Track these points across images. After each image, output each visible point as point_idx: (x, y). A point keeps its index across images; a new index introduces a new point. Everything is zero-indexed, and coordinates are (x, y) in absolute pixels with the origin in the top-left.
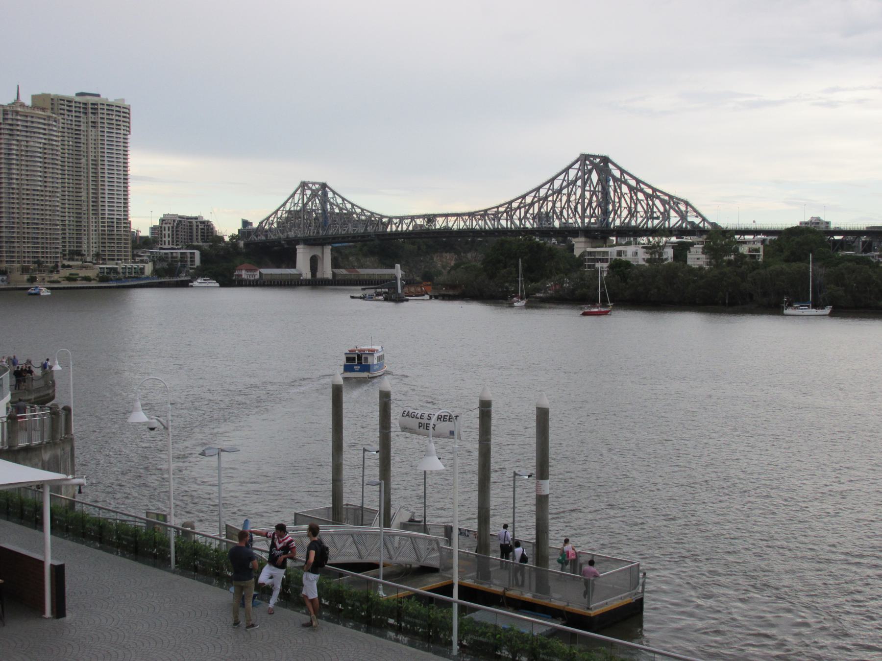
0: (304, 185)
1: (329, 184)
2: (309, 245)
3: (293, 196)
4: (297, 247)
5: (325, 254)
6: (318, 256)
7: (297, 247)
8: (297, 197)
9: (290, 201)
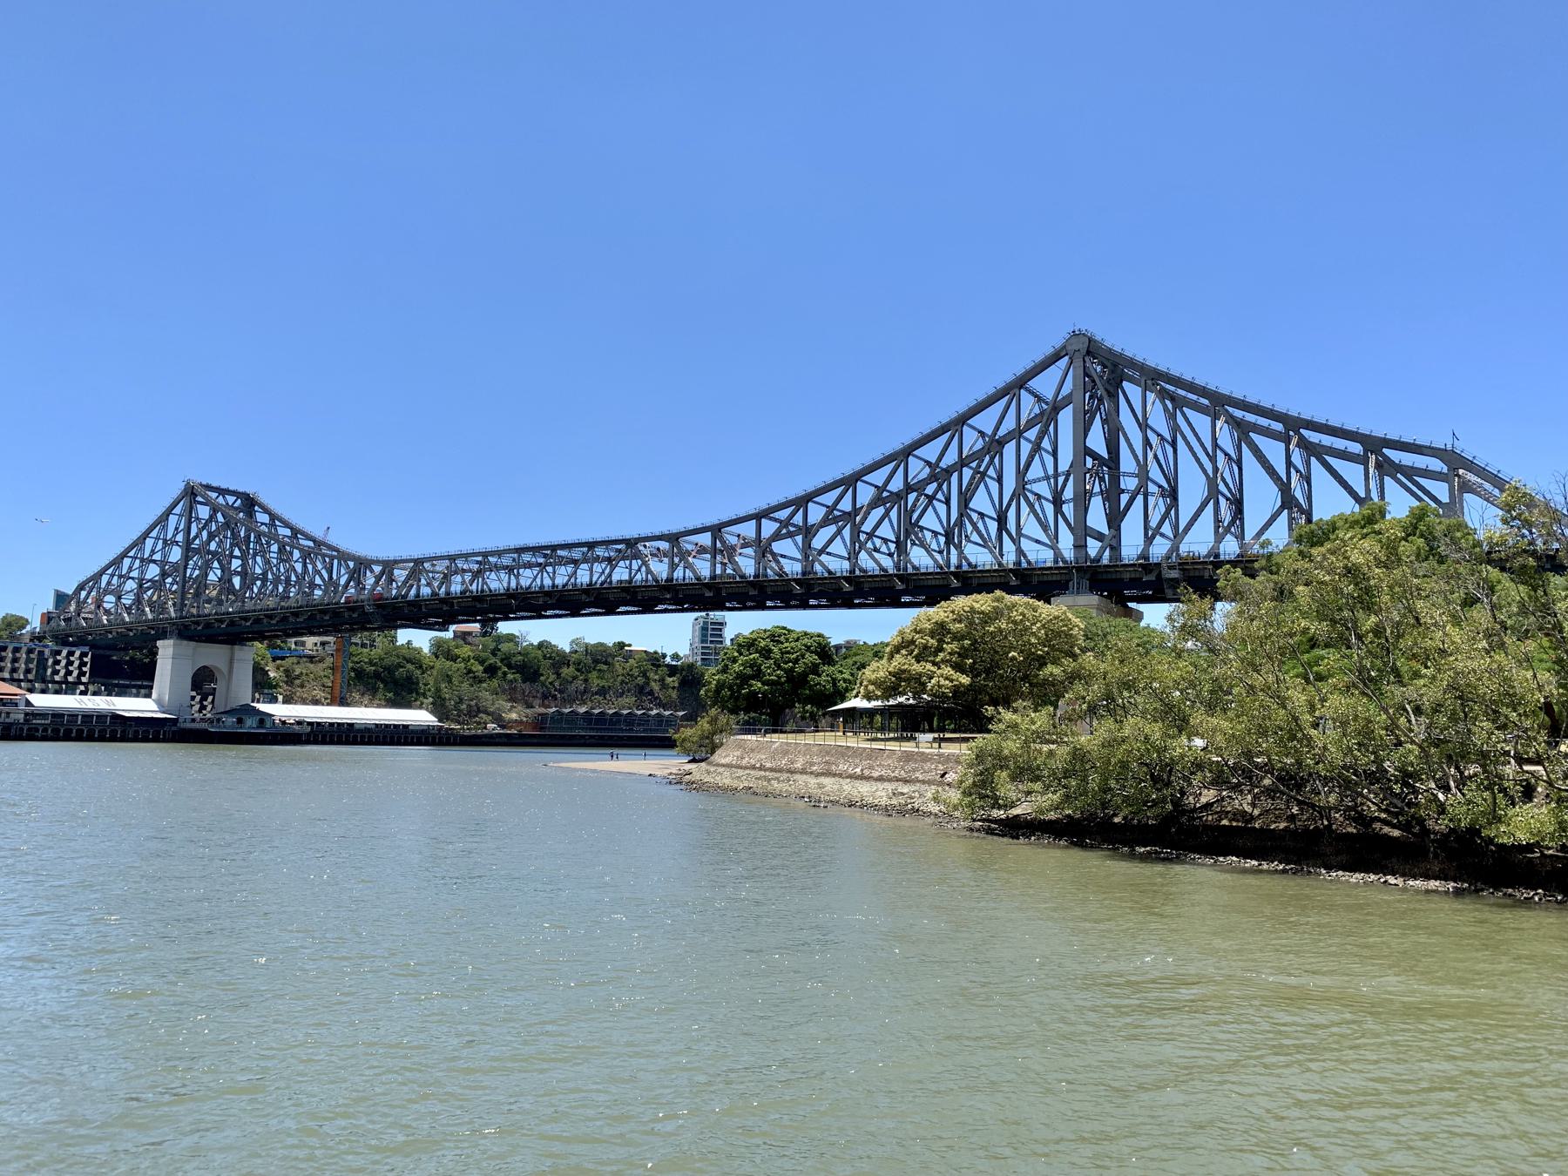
0: (191, 493)
1: (263, 498)
2: (190, 638)
3: (163, 520)
4: (159, 643)
5: (235, 665)
6: (219, 670)
7: (159, 643)
8: (173, 520)
9: (154, 534)
